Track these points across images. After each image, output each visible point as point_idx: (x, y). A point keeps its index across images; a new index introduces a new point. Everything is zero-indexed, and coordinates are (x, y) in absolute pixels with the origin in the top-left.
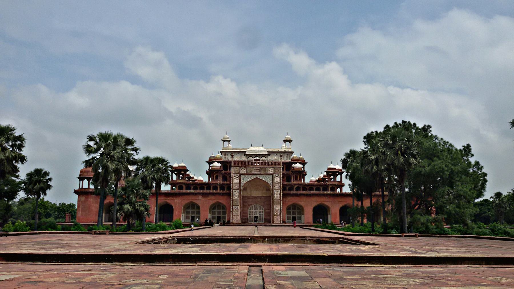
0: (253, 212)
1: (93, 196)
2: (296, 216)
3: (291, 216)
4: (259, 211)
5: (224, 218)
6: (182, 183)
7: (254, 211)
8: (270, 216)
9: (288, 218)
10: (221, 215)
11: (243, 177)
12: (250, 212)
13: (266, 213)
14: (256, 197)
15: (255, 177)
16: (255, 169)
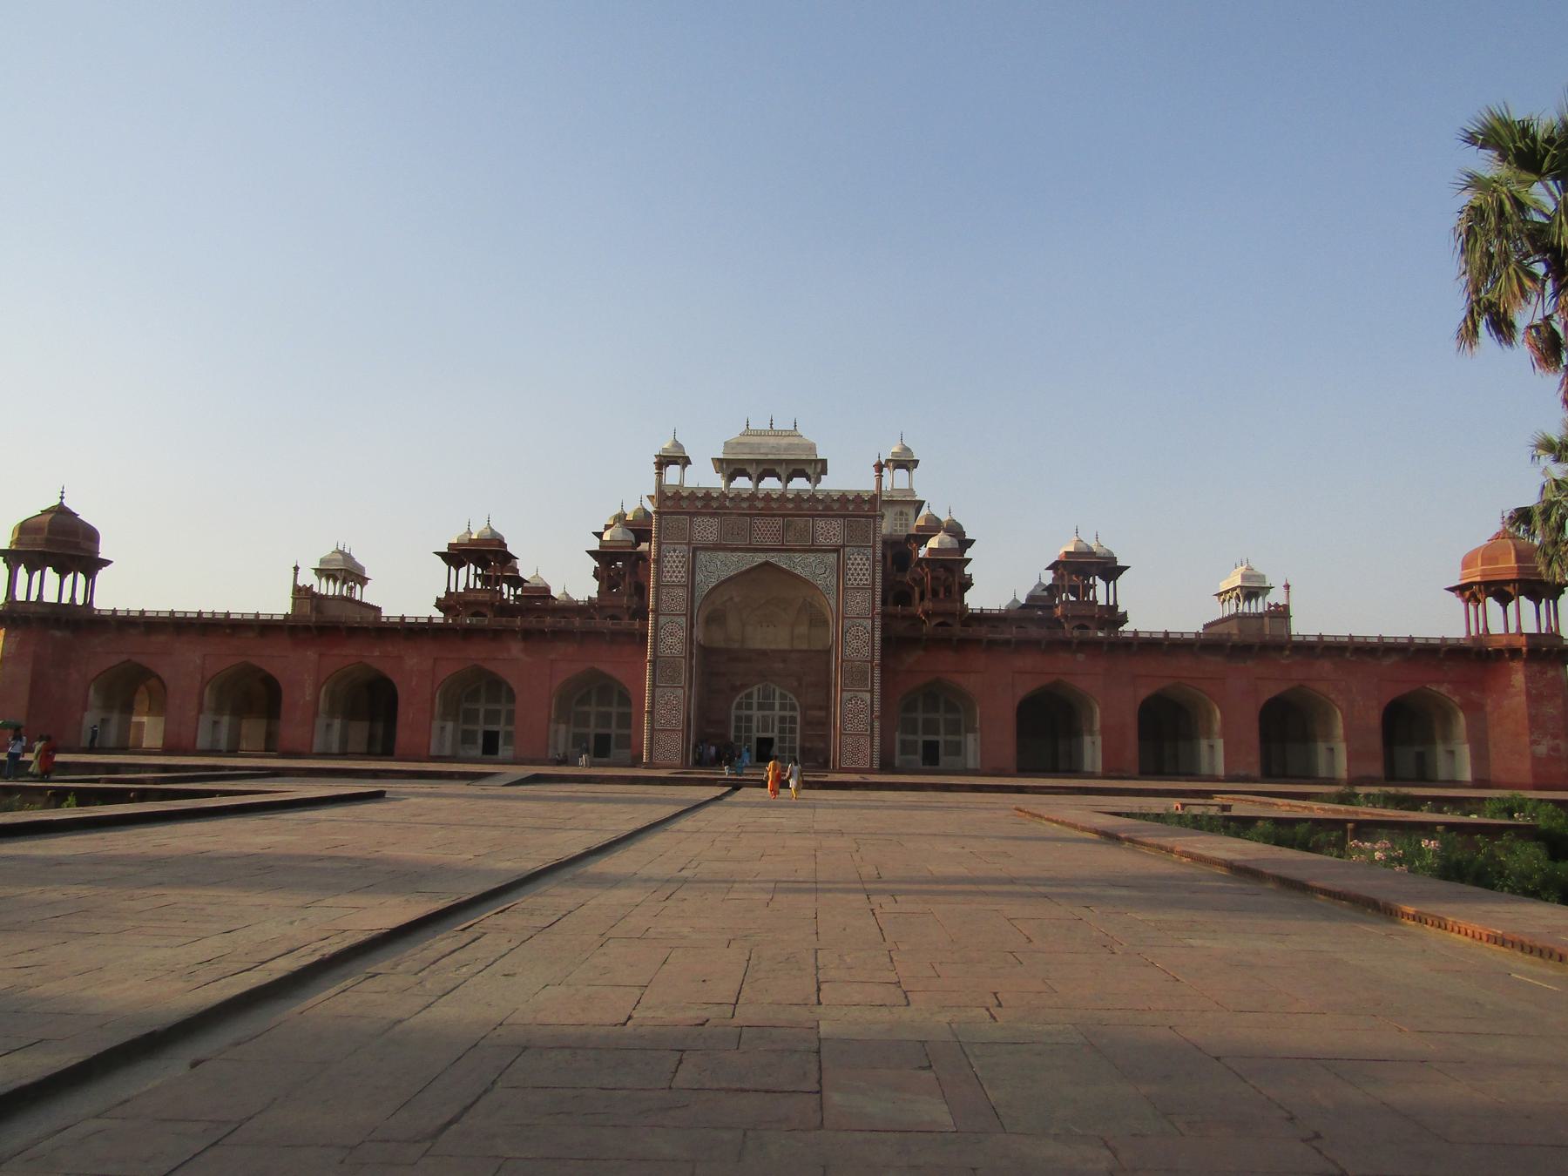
0: (749, 719)
1: (58, 634)
2: (941, 738)
3: (921, 738)
4: (777, 712)
5: (625, 742)
6: (483, 604)
7: (756, 714)
8: (826, 738)
9: (907, 748)
10: (614, 730)
11: (702, 557)
12: (739, 719)
13: (807, 723)
14: (763, 653)
15: (760, 558)
16: (758, 522)
